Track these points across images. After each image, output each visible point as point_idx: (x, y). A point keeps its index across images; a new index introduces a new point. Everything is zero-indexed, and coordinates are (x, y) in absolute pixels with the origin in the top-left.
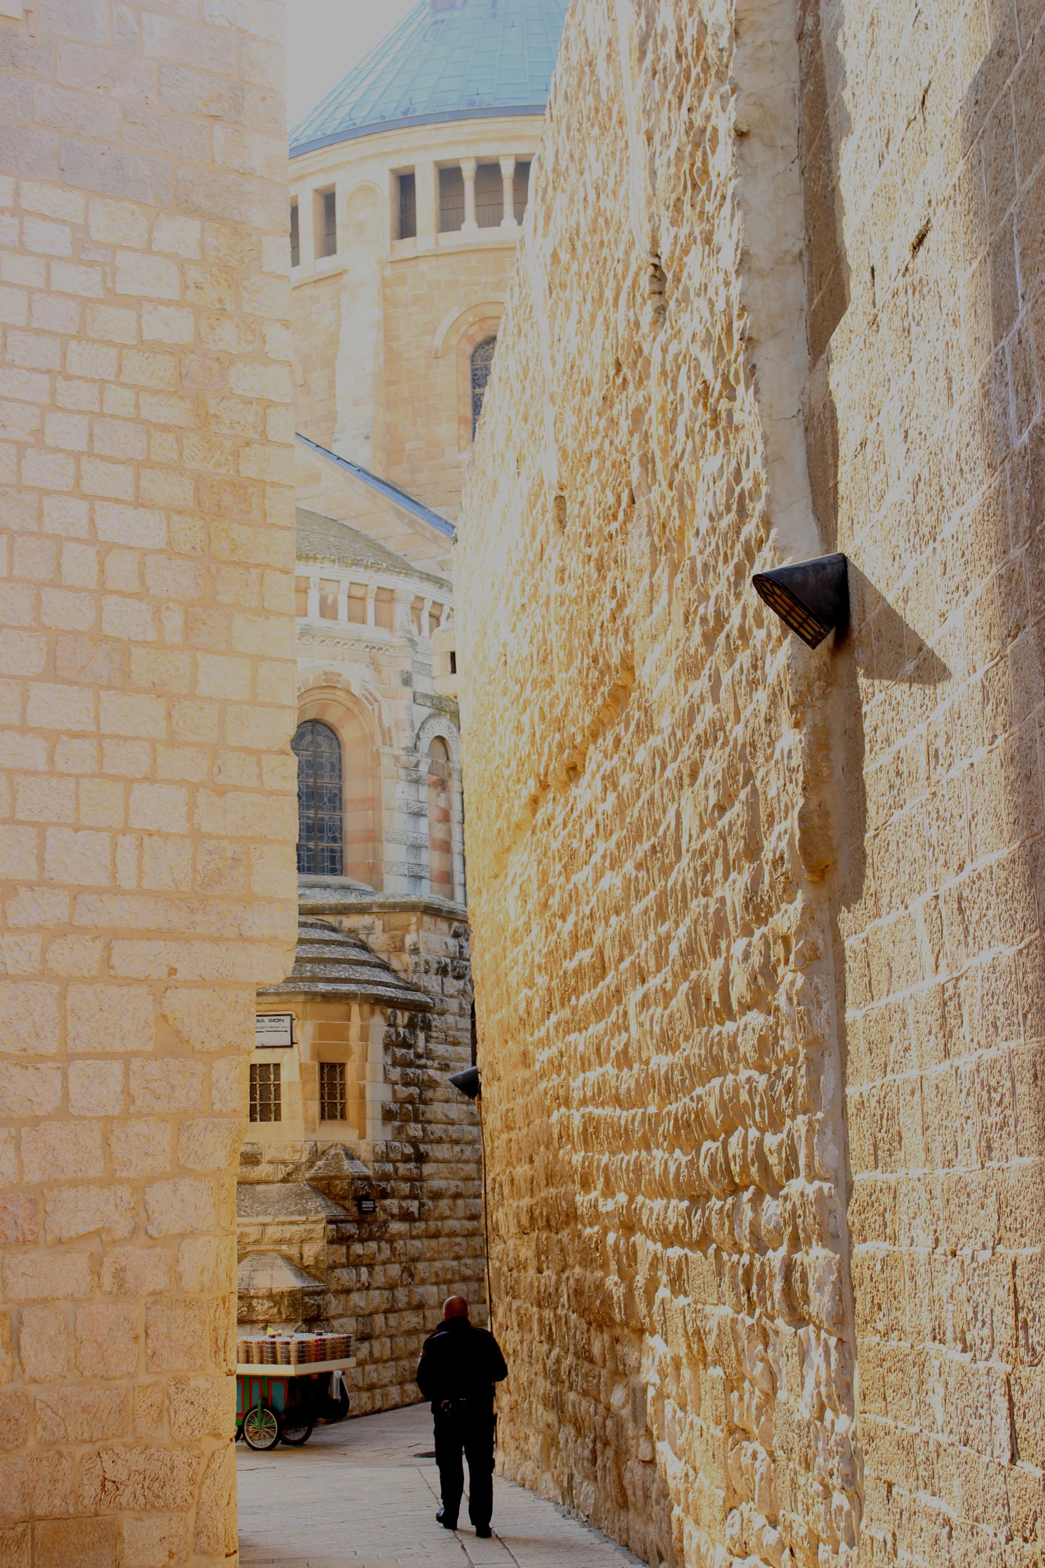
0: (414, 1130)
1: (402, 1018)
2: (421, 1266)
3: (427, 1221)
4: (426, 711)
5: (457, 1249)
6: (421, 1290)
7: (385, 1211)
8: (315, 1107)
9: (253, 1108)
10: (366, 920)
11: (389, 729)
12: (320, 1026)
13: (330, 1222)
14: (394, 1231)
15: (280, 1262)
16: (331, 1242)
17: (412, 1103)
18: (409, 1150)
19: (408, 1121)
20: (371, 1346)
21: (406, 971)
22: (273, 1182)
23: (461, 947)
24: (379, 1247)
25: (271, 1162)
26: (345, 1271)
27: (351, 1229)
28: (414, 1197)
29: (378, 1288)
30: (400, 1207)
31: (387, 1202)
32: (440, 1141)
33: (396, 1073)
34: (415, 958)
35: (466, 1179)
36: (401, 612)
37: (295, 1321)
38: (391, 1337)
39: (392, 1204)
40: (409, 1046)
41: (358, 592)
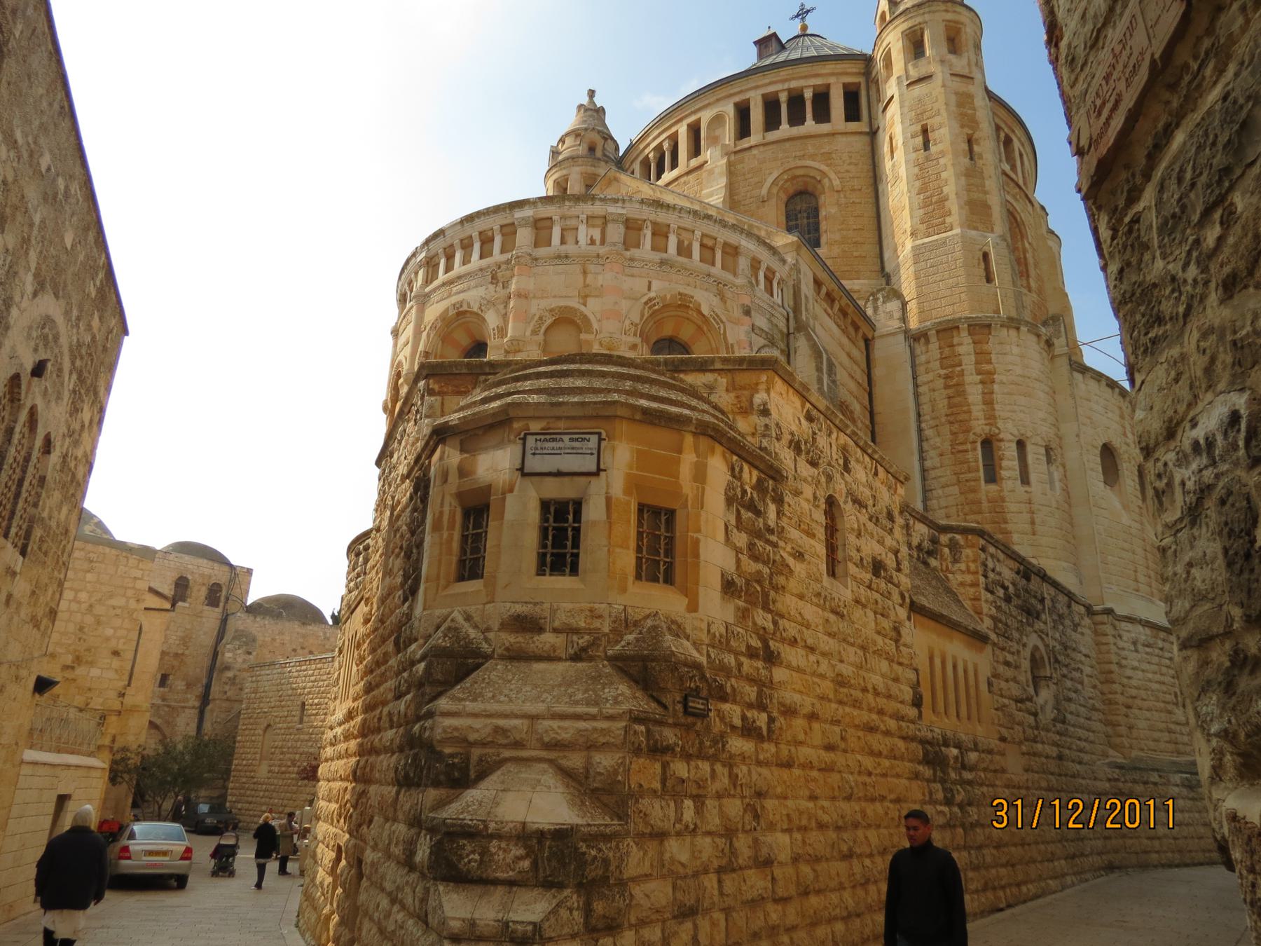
0: (762, 619)
1: (750, 476)
2: (770, 804)
3: (777, 744)
4: (762, 342)
5: (812, 785)
6: (769, 838)
7: (722, 719)
8: (627, 560)
9: (542, 558)
10: (708, 378)
11: (732, 345)
12: (638, 451)
13: (637, 720)
14: (733, 750)
15: (550, 778)
16: (637, 751)
17: (758, 582)
18: (755, 643)
19: (754, 604)
20: (696, 927)
21: (753, 434)
22: (559, 659)
23: (814, 433)
24: (713, 771)
25: (556, 631)
26: (657, 804)
27: (670, 736)
28: (761, 707)
29: (709, 833)
30: (744, 718)
31: (726, 707)
32: (793, 642)
33: (741, 539)
34: (762, 420)
35: (822, 698)
36: (743, 263)
37: (561, 886)
38: (727, 911)
39: (734, 712)
40: (758, 513)
41: (710, 243)
